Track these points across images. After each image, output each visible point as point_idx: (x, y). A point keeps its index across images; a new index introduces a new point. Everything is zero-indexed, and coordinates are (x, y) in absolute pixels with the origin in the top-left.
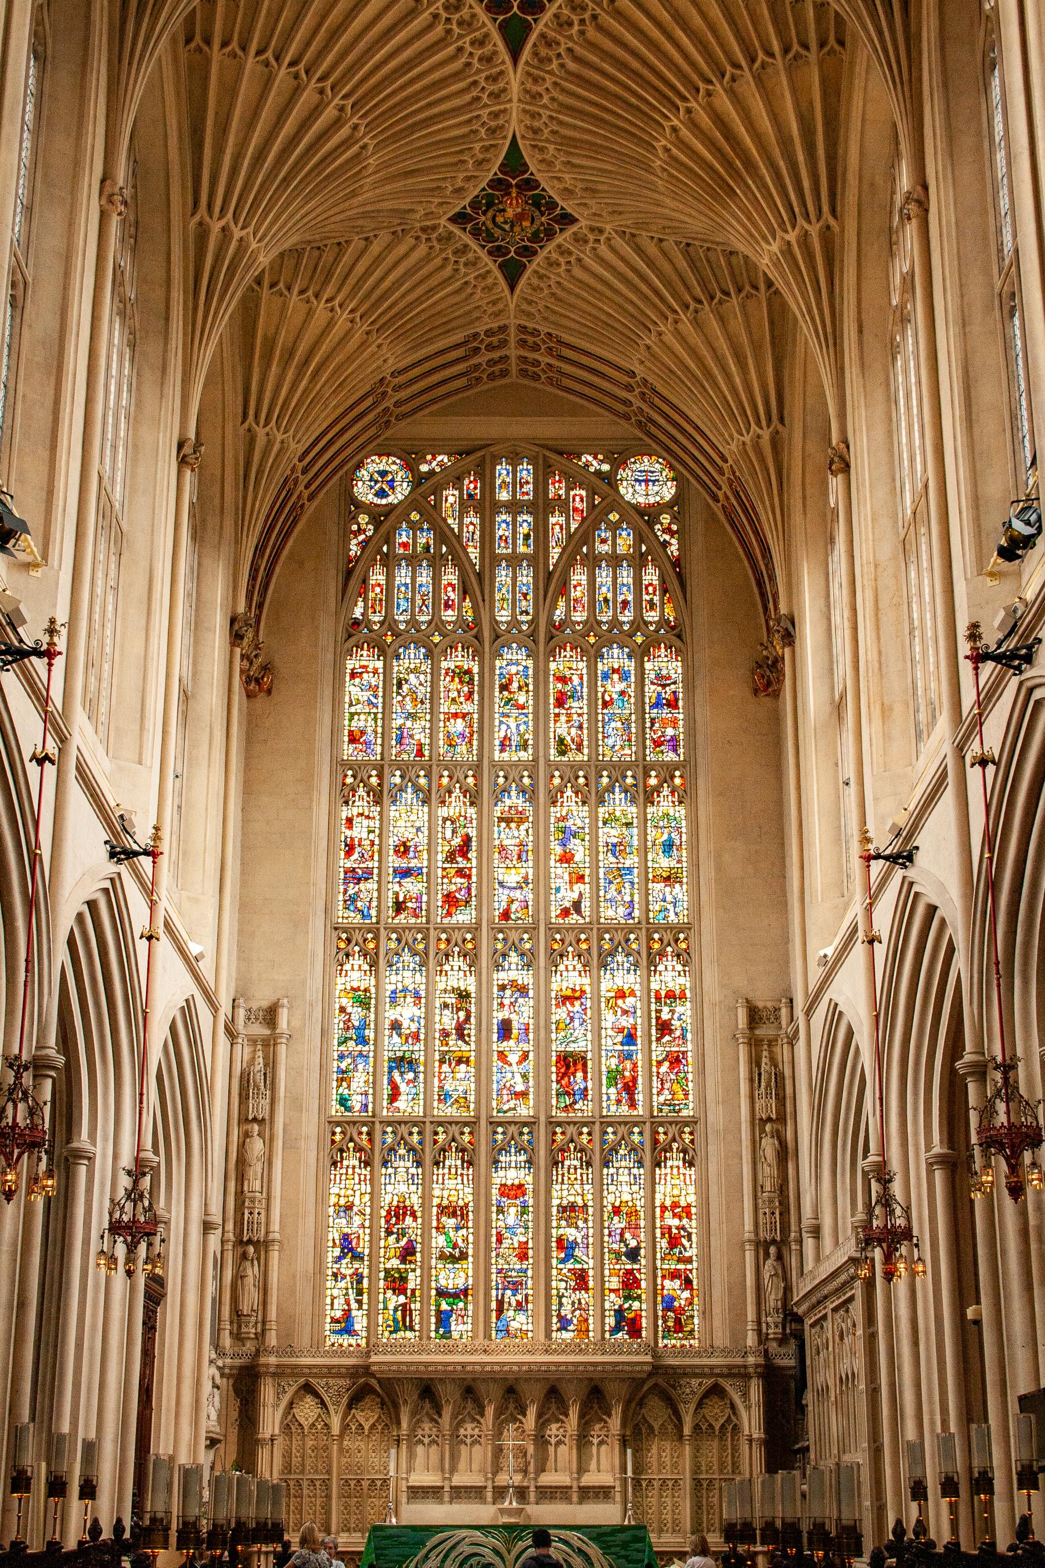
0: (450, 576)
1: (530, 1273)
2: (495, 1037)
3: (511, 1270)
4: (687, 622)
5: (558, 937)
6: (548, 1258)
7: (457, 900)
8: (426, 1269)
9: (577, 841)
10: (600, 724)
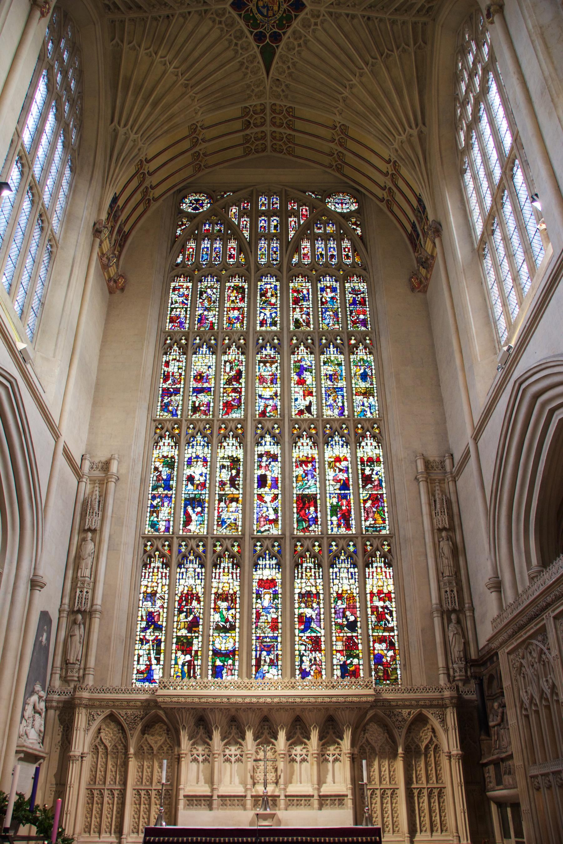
0: (233, 244)
1: (279, 639)
3: (266, 637)
4: (369, 263)
5: (297, 426)
6: (293, 629)
7: (233, 406)
9: (308, 373)
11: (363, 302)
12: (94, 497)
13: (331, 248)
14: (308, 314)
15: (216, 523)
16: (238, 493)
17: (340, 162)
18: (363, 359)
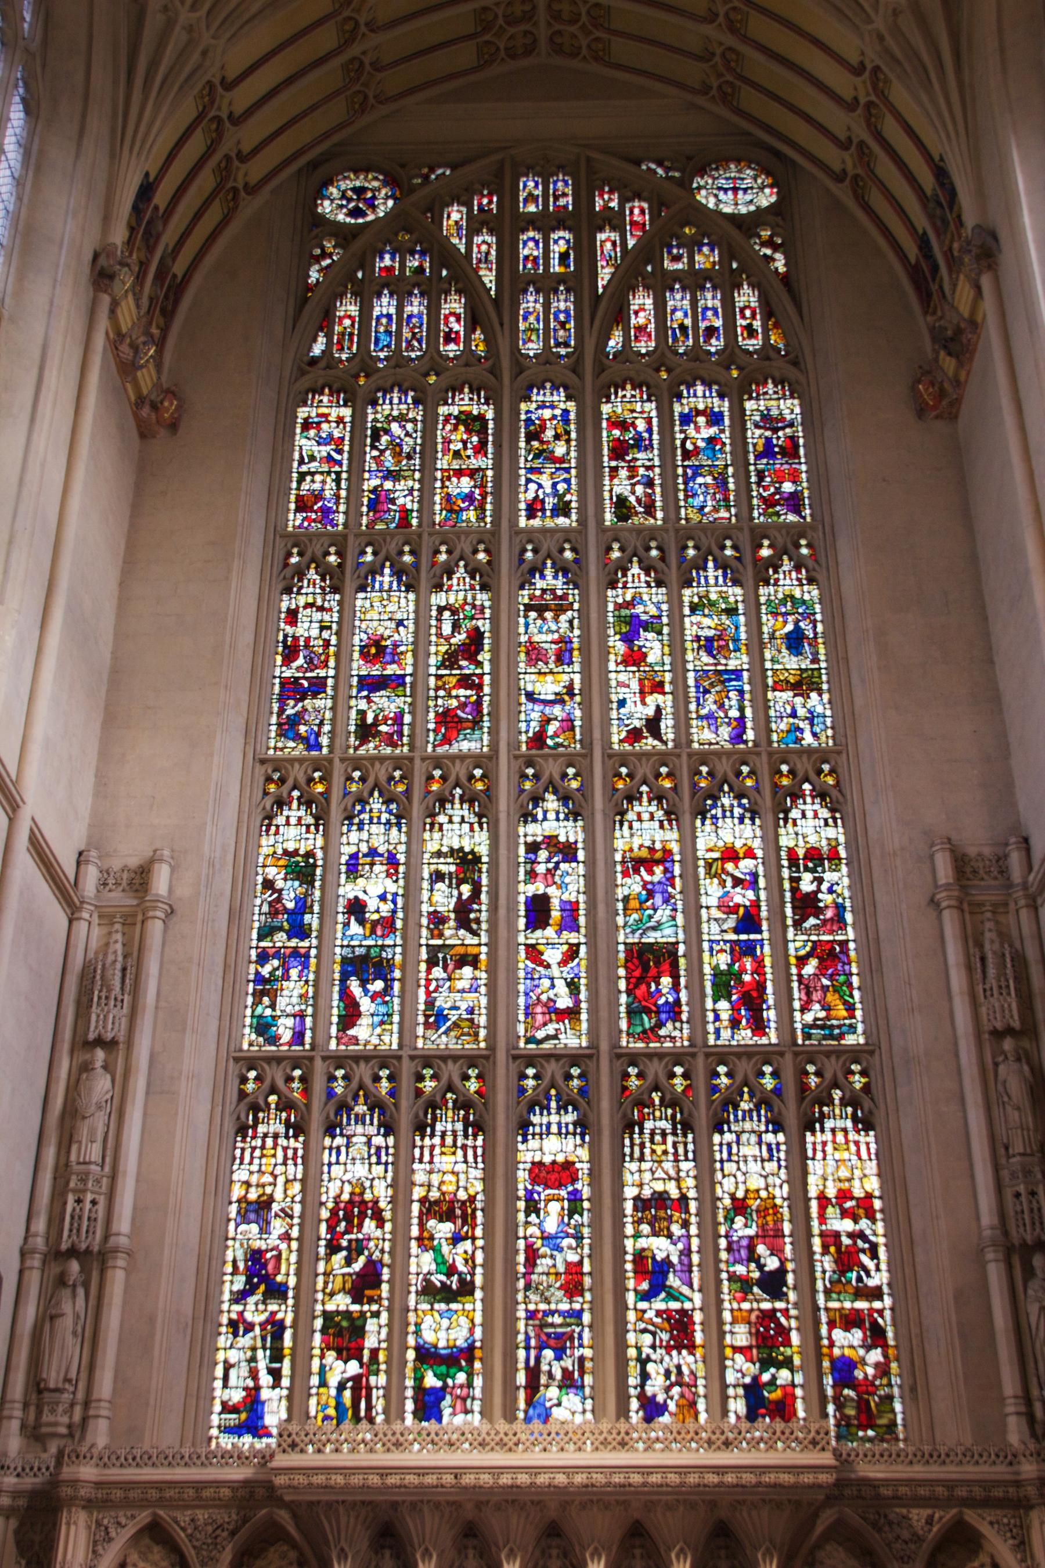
0: (454, 304)
1: (586, 1318)
2: (522, 922)
3: (552, 1313)
5: (624, 770)
6: (620, 1290)
7: (461, 720)
8: (399, 1314)
9: (651, 635)
10: (680, 480)
11: (790, 450)
12: (111, 958)
13: (706, 309)
14: (650, 483)
15: (421, 1019)
16: (477, 942)
17: (729, 77)
18: (792, 597)
